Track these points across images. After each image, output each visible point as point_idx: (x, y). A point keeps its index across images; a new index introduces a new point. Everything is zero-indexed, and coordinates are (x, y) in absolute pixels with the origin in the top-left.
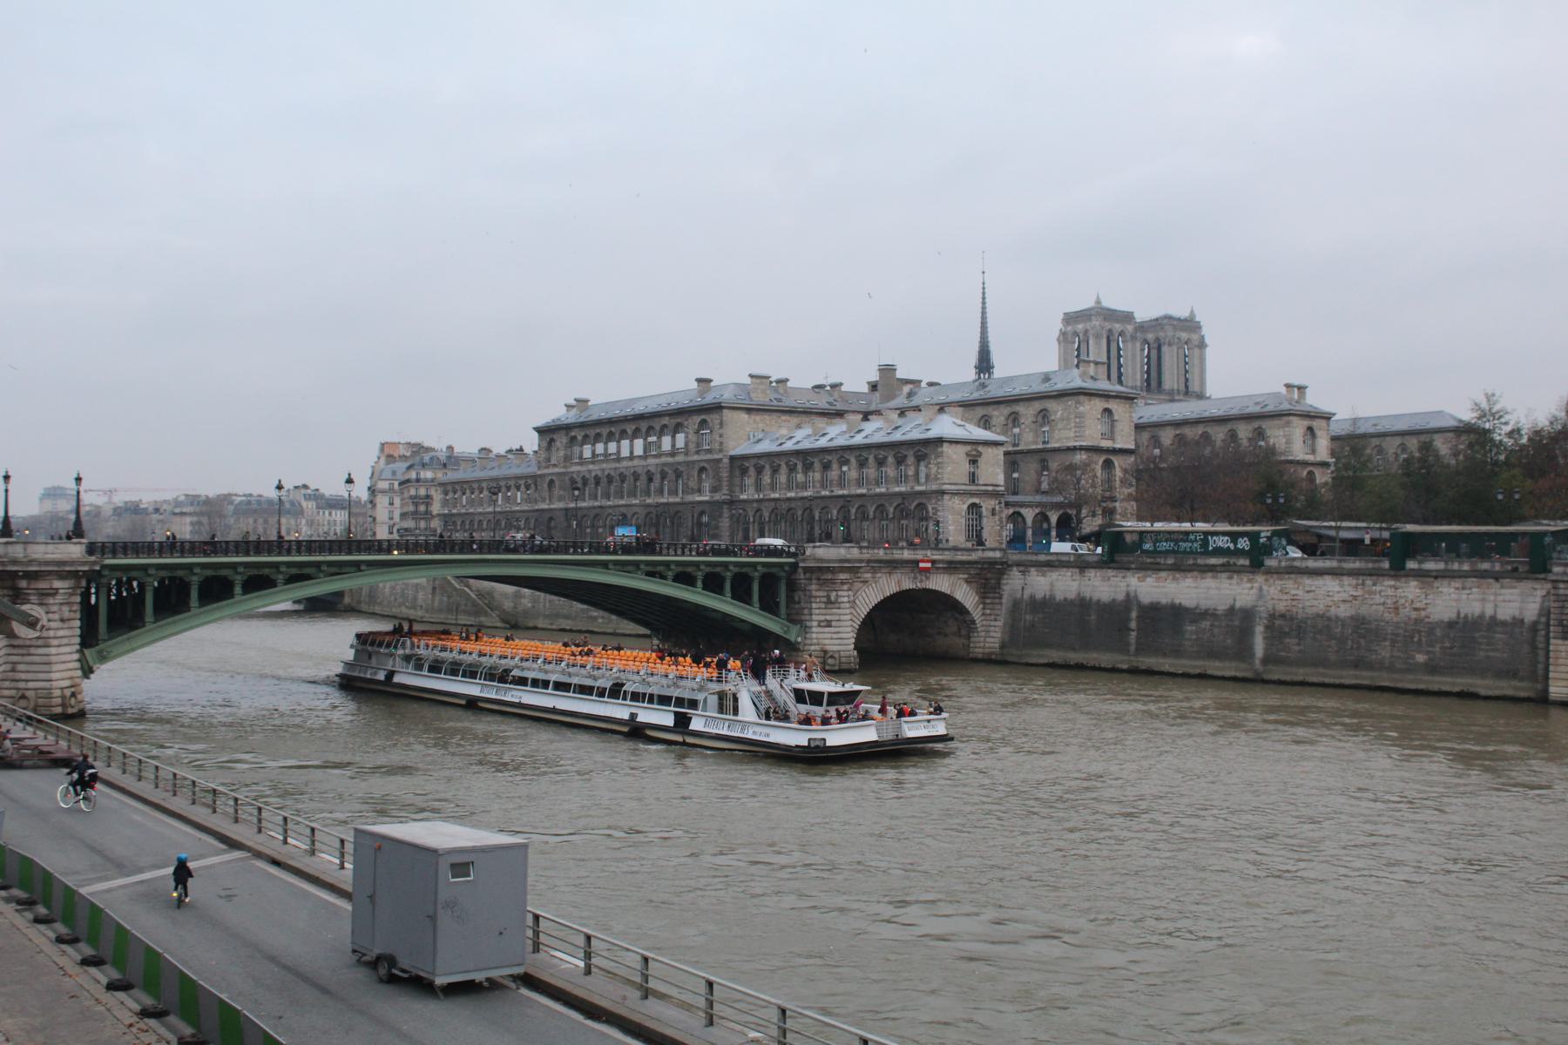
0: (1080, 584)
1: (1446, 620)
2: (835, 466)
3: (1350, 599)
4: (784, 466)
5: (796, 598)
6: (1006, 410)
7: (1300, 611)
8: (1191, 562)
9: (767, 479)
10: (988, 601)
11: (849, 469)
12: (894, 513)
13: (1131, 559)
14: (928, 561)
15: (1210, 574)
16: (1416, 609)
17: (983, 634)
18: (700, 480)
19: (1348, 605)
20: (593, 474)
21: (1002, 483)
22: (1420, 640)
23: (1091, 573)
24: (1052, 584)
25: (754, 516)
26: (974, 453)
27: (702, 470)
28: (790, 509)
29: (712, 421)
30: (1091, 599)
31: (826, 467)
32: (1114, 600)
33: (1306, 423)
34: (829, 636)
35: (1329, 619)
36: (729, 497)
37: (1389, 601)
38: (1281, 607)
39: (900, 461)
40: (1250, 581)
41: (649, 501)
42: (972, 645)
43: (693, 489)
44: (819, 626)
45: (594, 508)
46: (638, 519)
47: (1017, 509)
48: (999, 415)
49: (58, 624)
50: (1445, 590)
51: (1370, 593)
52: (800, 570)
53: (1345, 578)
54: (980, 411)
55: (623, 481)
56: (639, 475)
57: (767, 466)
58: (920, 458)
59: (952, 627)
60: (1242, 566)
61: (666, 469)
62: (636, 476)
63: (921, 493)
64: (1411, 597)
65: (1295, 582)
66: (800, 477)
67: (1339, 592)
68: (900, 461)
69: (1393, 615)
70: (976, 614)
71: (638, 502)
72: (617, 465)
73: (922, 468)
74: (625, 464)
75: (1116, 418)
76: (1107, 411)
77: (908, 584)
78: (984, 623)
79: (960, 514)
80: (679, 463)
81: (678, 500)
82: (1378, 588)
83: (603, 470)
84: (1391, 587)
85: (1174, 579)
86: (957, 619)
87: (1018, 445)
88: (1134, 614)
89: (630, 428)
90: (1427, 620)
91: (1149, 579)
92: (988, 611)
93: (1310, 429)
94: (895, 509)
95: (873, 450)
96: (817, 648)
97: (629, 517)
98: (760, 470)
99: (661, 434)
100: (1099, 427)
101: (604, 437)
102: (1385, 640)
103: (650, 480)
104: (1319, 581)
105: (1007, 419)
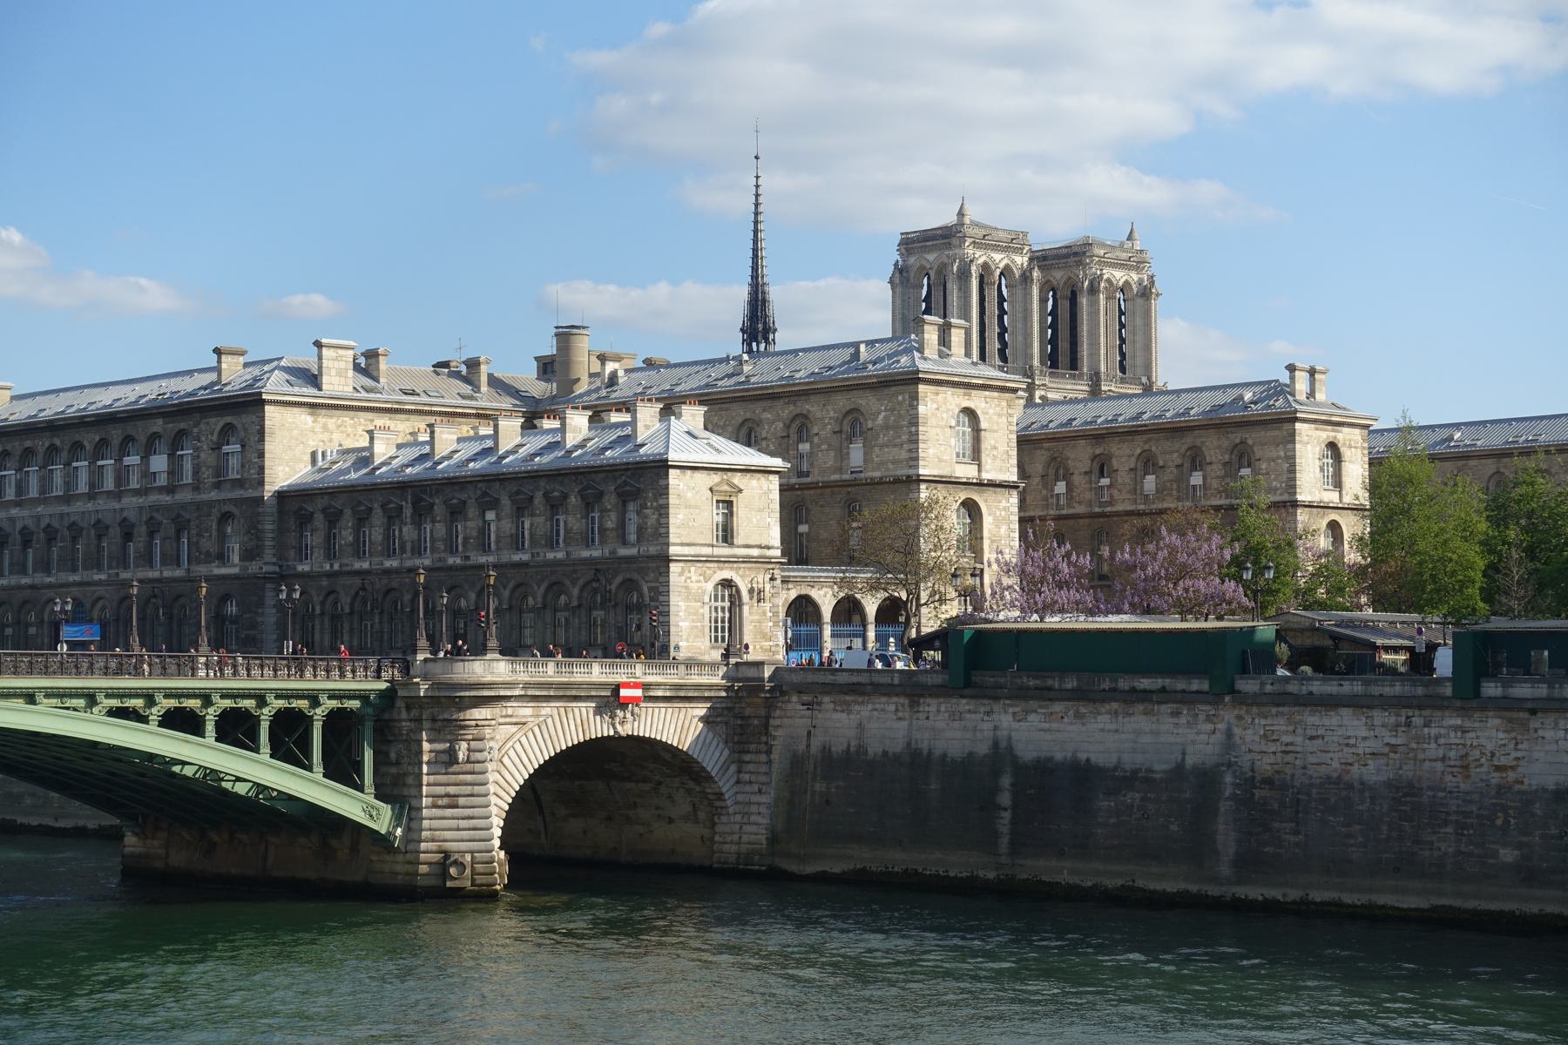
0: (910, 725)
1: (1552, 788)
2: (472, 511)
3: (1386, 750)
4: (378, 511)
5: (393, 756)
6: (787, 411)
7: (1299, 772)
8: (1106, 685)
9: (346, 535)
10: (747, 758)
11: (498, 518)
12: (580, 598)
13: (1002, 680)
14: (636, 686)
15: (1141, 707)
16: (1498, 768)
17: (738, 818)
18: (222, 537)
19: (1383, 761)
20: (19, 526)
21: (777, 542)
22: (1507, 822)
23: (931, 705)
24: (860, 726)
25: (323, 604)
26: (726, 488)
27: (225, 517)
28: (389, 591)
29: (246, 430)
30: (930, 753)
31: (456, 513)
32: (971, 754)
33: (1326, 434)
34: (453, 823)
35: (1350, 787)
36: (277, 569)
37: (1452, 754)
38: (1265, 765)
39: (591, 501)
40: (1209, 719)
41: (125, 575)
42: (717, 838)
43: (208, 554)
44: (435, 806)
45: (20, 587)
46: (103, 608)
47: (805, 590)
48: (773, 419)
50: (1549, 734)
51: (1419, 739)
52: (400, 704)
53: (1376, 713)
54: (740, 413)
55: (74, 539)
56: (107, 528)
57: (348, 512)
58: (625, 498)
59: (683, 806)
60: (1197, 692)
61: (158, 517)
62: (101, 528)
63: (629, 560)
64: (1490, 746)
65: (1290, 721)
66: (408, 532)
67: (1365, 738)
68: (591, 501)
69: (1460, 778)
70: (726, 785)
71: (103, 577)
72: (65, 509)
73: (632, 517)
74: (79, 506)
75: (983, 425)
76: (970, 413)
77: (600, 728)
78: (740, 798)
79: (699, 599)
80: (183, 506)
81: (179, 573)
82: (1434, 731)
83: (38, 518)
84: (1456, 728)
85: (1079, 716)
86: (689, 791)
87: (807, 474)
88: (1006, 781)
89: (89, 439)
90: (1517, 787)
91: (1032, 717)
92: (746, 777)
93: (1333, 446)
94: (582, 590)
95: (542, 483)
96: (431, 846)
97: (88, 606)
98: (333, 518)
99: (148, 451)
100: (953, 441)
101: (40, 456)
102: (1446, 823)
103: (128, 536)
104: (1332, 719)
105: (788, 427)
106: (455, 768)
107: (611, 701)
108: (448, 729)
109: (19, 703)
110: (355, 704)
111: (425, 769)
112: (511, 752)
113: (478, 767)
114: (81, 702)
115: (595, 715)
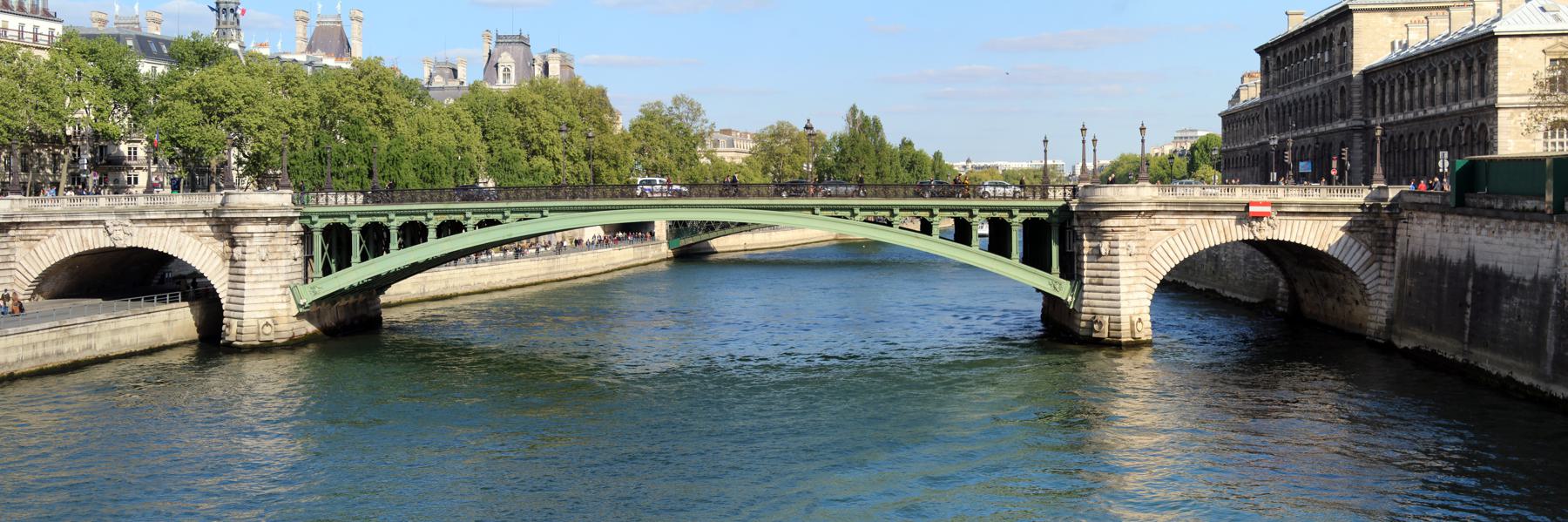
44: (1091, 283)
49: (259, 263)
70: (1367, 278)
77: (1242, 233)
106: (1102, 259)
107: (1245, 215)
108: (1097, 234)
109: (809, 213)
110: (1045, 216)
111: (1085, 258)
112: (1160, 250)
113: (1114, 258)
114: (848, 214)
115: (1236, 224)
